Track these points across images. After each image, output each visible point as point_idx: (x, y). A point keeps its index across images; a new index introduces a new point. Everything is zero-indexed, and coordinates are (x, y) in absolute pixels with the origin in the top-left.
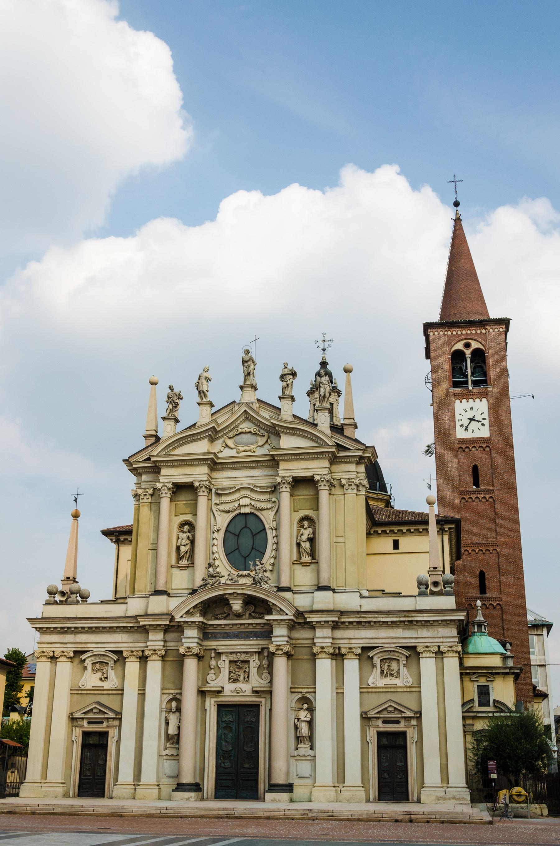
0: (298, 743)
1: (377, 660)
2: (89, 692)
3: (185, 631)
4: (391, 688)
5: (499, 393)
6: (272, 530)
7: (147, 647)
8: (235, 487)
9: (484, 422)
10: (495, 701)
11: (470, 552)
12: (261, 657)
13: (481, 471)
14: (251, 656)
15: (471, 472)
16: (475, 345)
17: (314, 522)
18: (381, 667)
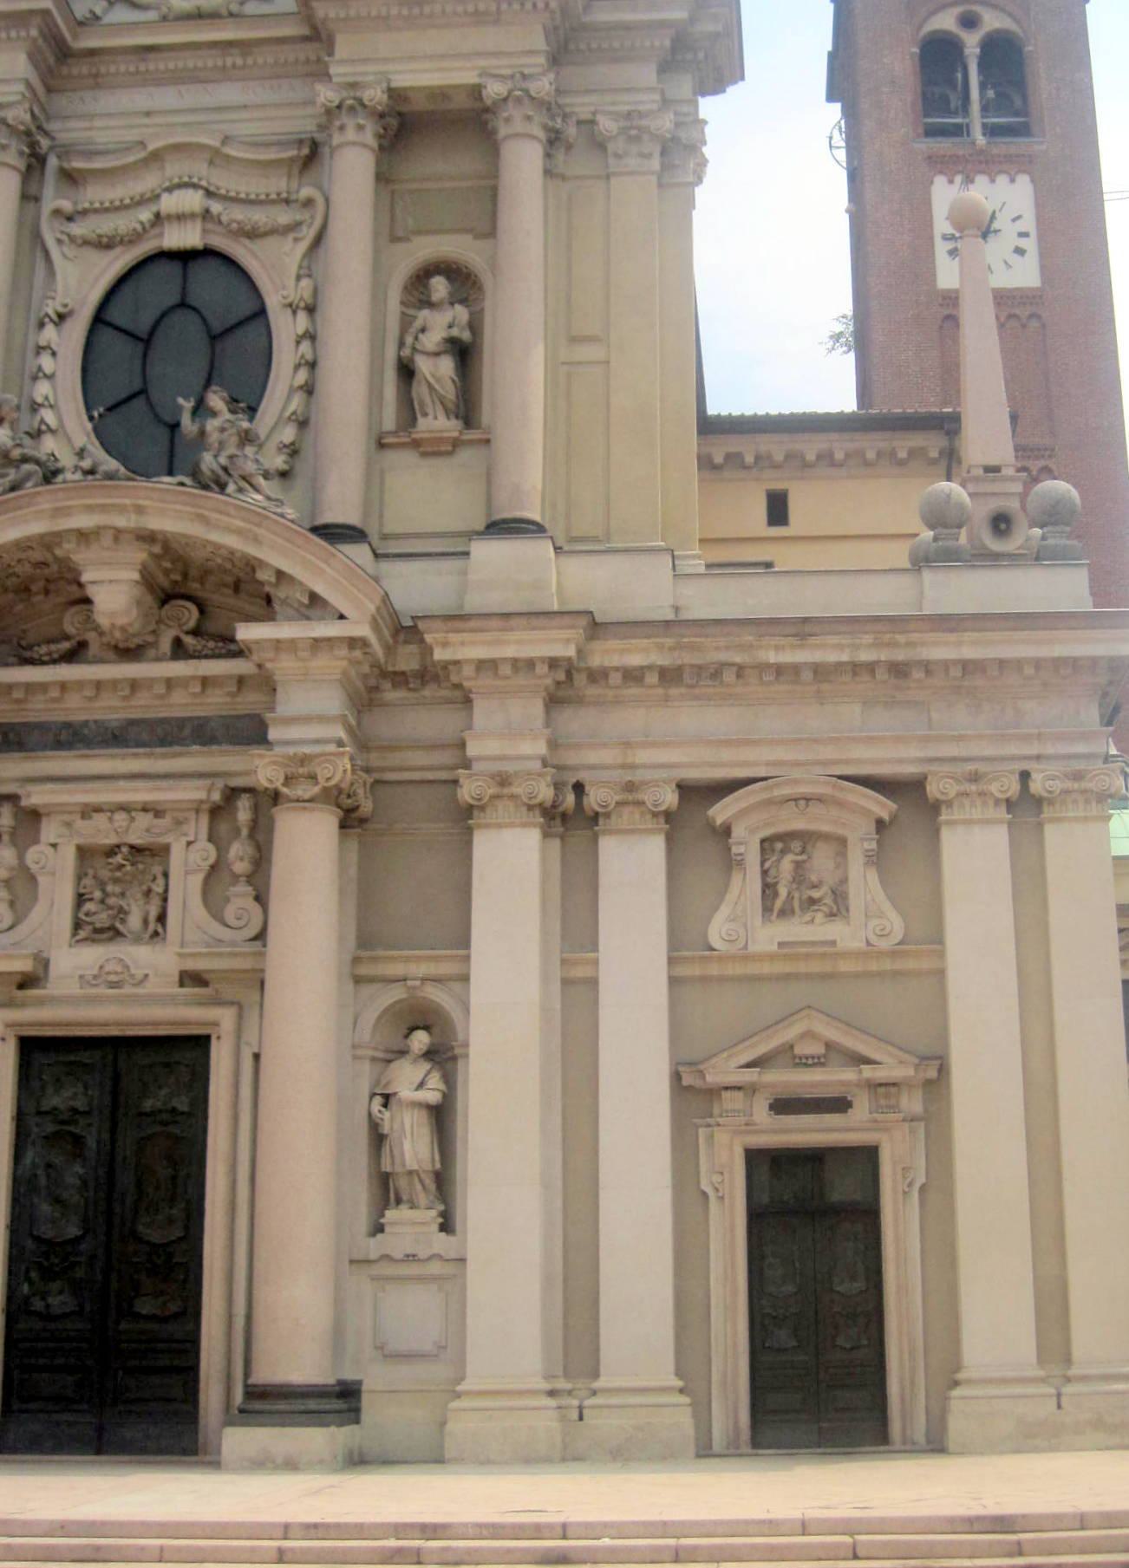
0: (385, 1204)
1: (746, 842)
4: (807, 956)
6: (294, 313)
8: (142, 144)
9: (1023, 243)
12: (223, 828)
14: (178, 823)
17: (475, 283)
18: (765, 873)
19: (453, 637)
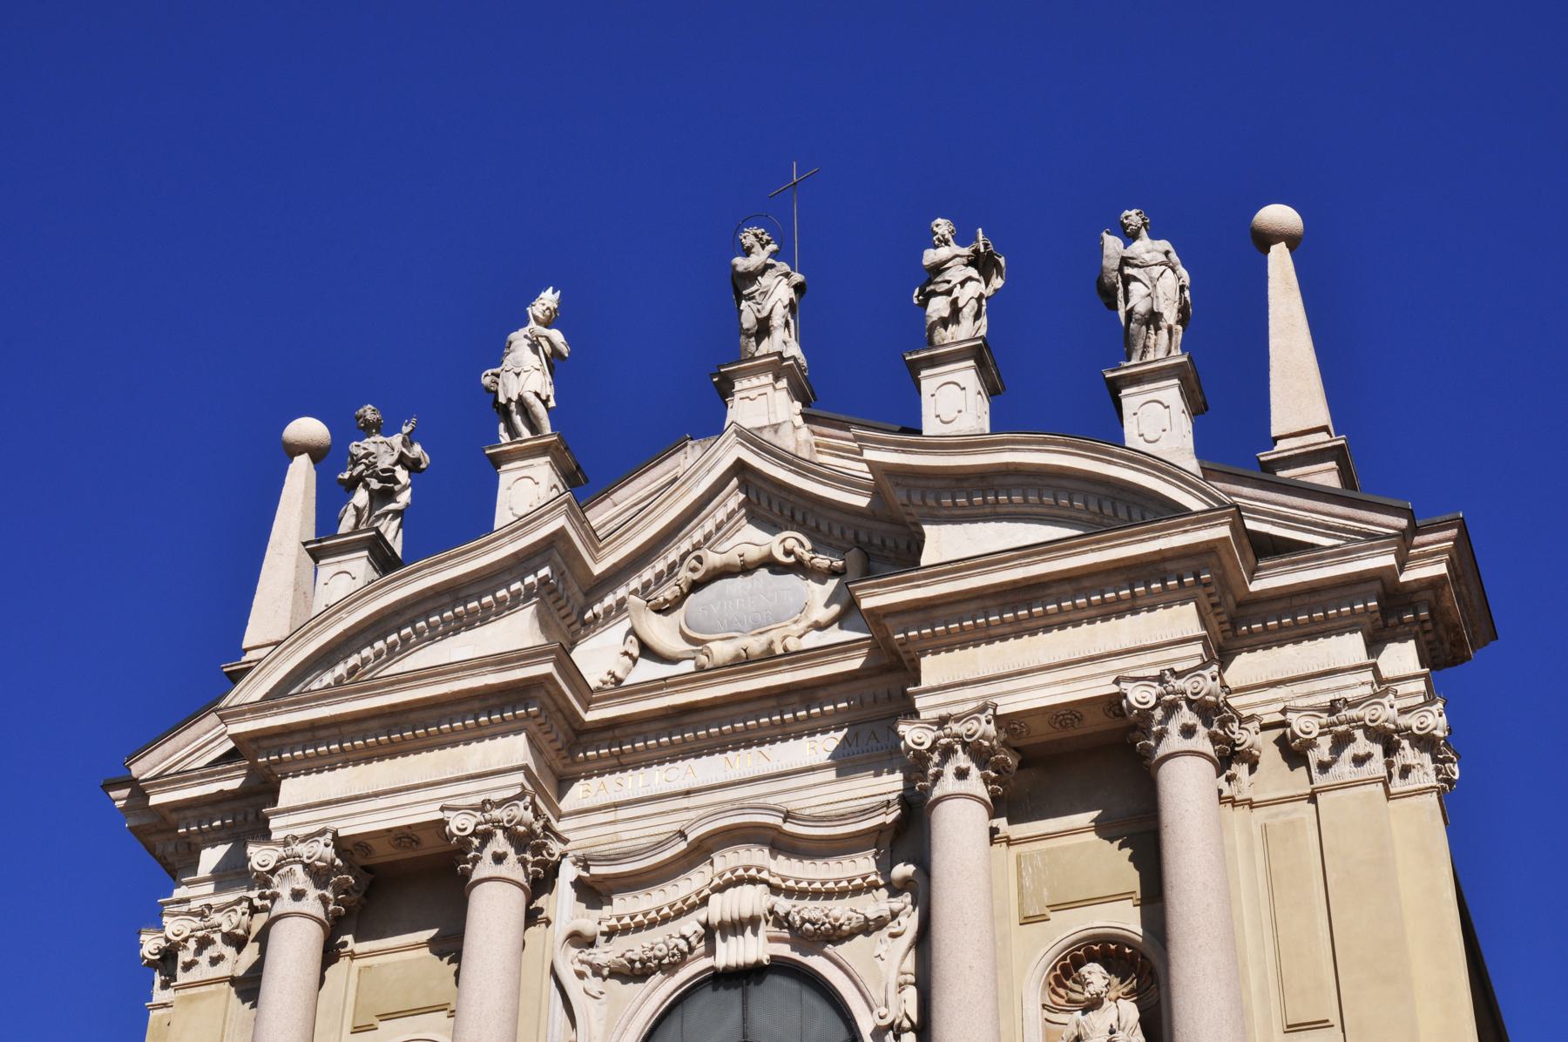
8: (682, 834)
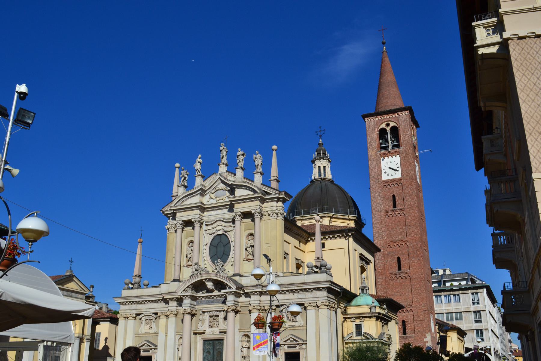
2: (143, 335)
3: (184, 300)
5: (407, 151)
7: (168, 310)
9: (398, 169)
10: (364, 333)
11: (391, 246)
13: (397, 198)
15: (391, 199)
16: (392, 124)
19: (247, 289)
